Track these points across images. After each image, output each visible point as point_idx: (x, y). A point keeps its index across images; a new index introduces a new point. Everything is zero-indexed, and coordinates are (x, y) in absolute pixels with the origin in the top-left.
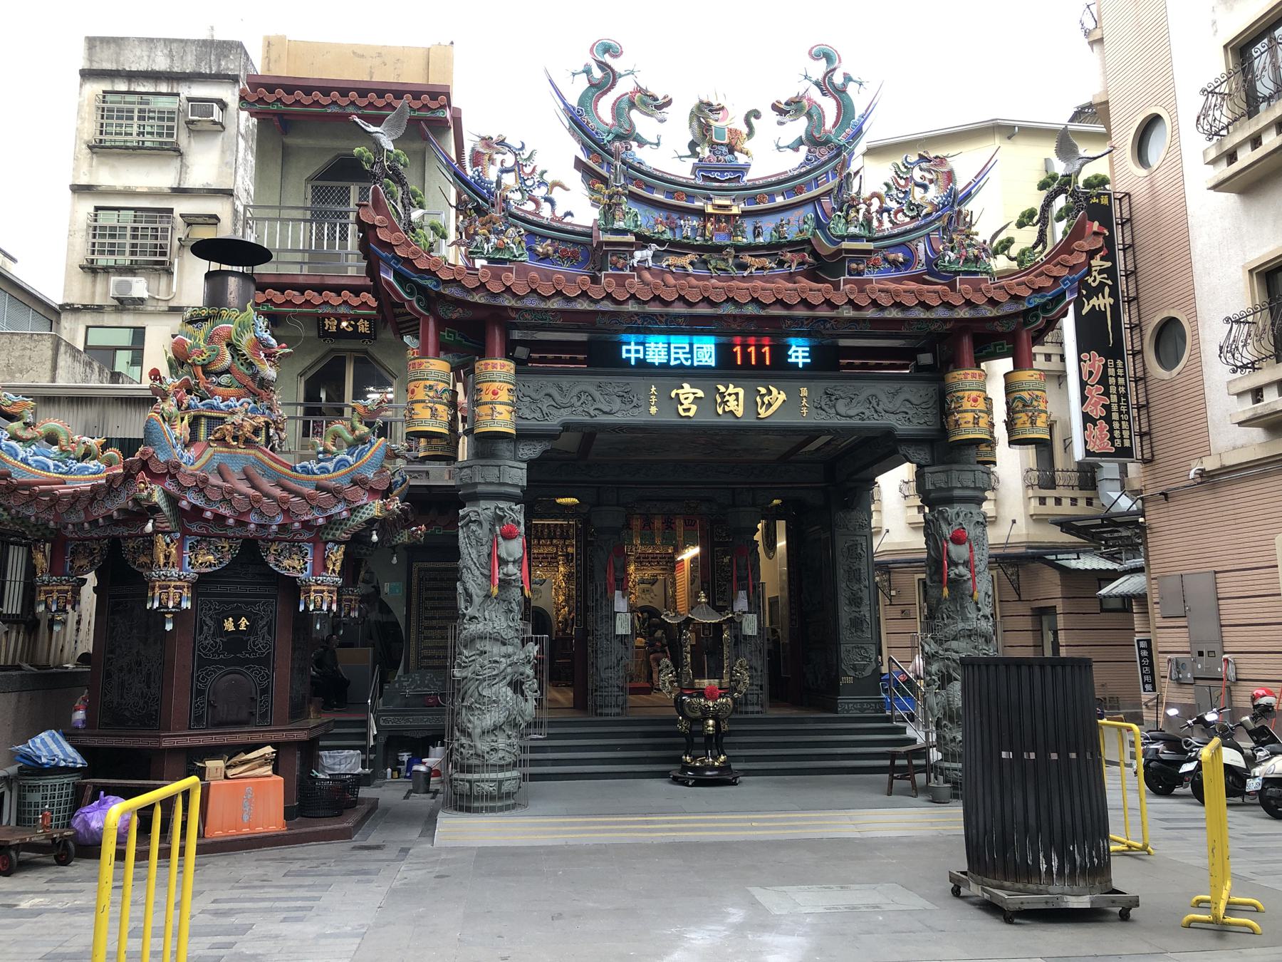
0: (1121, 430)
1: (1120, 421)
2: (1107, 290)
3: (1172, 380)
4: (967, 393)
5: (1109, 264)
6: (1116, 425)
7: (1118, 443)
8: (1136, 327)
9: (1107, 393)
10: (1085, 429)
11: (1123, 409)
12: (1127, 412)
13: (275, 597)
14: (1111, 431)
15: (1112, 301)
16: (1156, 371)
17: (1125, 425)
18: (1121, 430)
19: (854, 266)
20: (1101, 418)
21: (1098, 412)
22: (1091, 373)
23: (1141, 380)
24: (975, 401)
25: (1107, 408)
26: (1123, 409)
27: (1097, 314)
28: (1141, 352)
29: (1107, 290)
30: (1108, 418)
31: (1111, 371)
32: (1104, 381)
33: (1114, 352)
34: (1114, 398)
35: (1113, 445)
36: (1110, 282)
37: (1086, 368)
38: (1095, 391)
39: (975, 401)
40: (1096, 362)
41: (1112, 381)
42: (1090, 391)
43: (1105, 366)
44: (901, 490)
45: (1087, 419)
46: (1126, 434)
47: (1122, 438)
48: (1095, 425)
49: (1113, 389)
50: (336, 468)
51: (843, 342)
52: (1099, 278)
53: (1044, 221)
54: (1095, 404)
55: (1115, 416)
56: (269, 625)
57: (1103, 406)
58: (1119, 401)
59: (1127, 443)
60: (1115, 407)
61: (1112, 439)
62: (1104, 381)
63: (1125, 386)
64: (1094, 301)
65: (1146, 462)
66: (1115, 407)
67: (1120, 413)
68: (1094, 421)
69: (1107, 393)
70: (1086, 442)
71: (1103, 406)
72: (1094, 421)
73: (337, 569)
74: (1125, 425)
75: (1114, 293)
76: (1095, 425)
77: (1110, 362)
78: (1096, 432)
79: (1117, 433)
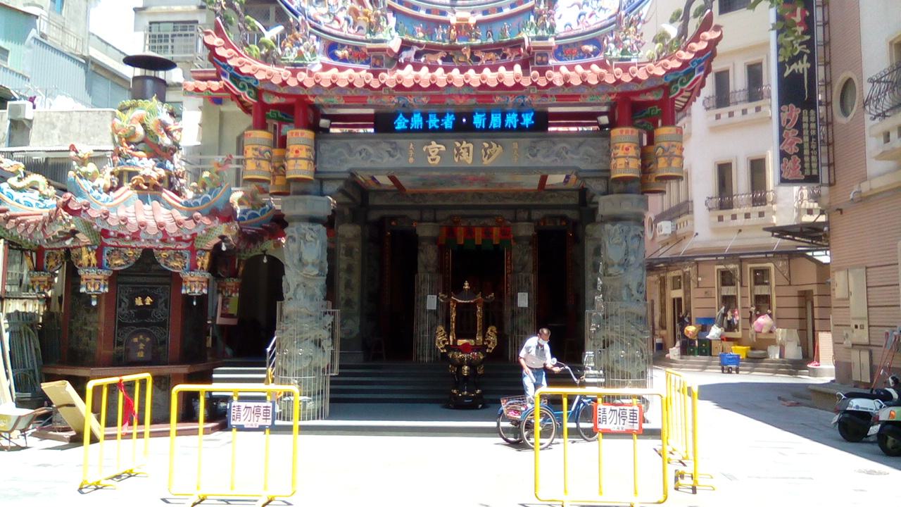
0: (810, 162)
1: (810, 155)
2: (805, 57)
3: (848, 125)
4: (622, 144)
5: (807, 37)
6: (807, 159)
7: (807, 172)
8: (828, 84)
9: (800, 135)
10: (781, 162)
11: (814, 147)
12: (817, 149)
13: (169, 284)
14: (803, 163)
15: (809, 65)
16: (840, 119)
17: (814, 158)
18: (810, 162)
19: (539, 58)
20: (795, 154)
21: (793, 149)
22: (788, 121)
23: (829, 123)
24: (627, 149)
25: (801, 146)
26: (814, 147)
27: (796, 77)
28: (831, 103)
29: (805, 57)
30: (800, 154)
31: (805, 119)
32: (799, 126)
33: (810, 104)
34: (806, 139)
35: (803, 174)
36: (808, 51)
37: (785, 116)
38: (791, 134)
39: (627, 149)
40: (794, 111)
41: (805, 126)
42: (787, 134)
43: (801, 116)
45: (783, 155)
46: (814, 165)
47: (811, 168)
48: (789, 159)
49: (806, 132)
50: (202, 203)
51: (551, 110)
52: (799, 49)
53: (686, 19)
54: (791, 144)
55: (806, 152)
56: (166, 302)
57: (797, 145)
58: (810, 140)
59: (815, 172)
60: (806, 146)
61: (803, 169)
62: (799, 126)
63: (816, 129)
64: (794, 66)
65: (830, 185)
66: (806, 146)
67: (811, 150)
68: (789, 157)
69: (800, 135)
70: (781, 172)
71: (797, 145)
72: (789, 157)
73: (205, 266)
74: (814, 158)
75: (811, 59)
76: (789, 159)
77: (805, 112)
78: (790, 164)
79: (807, 165)
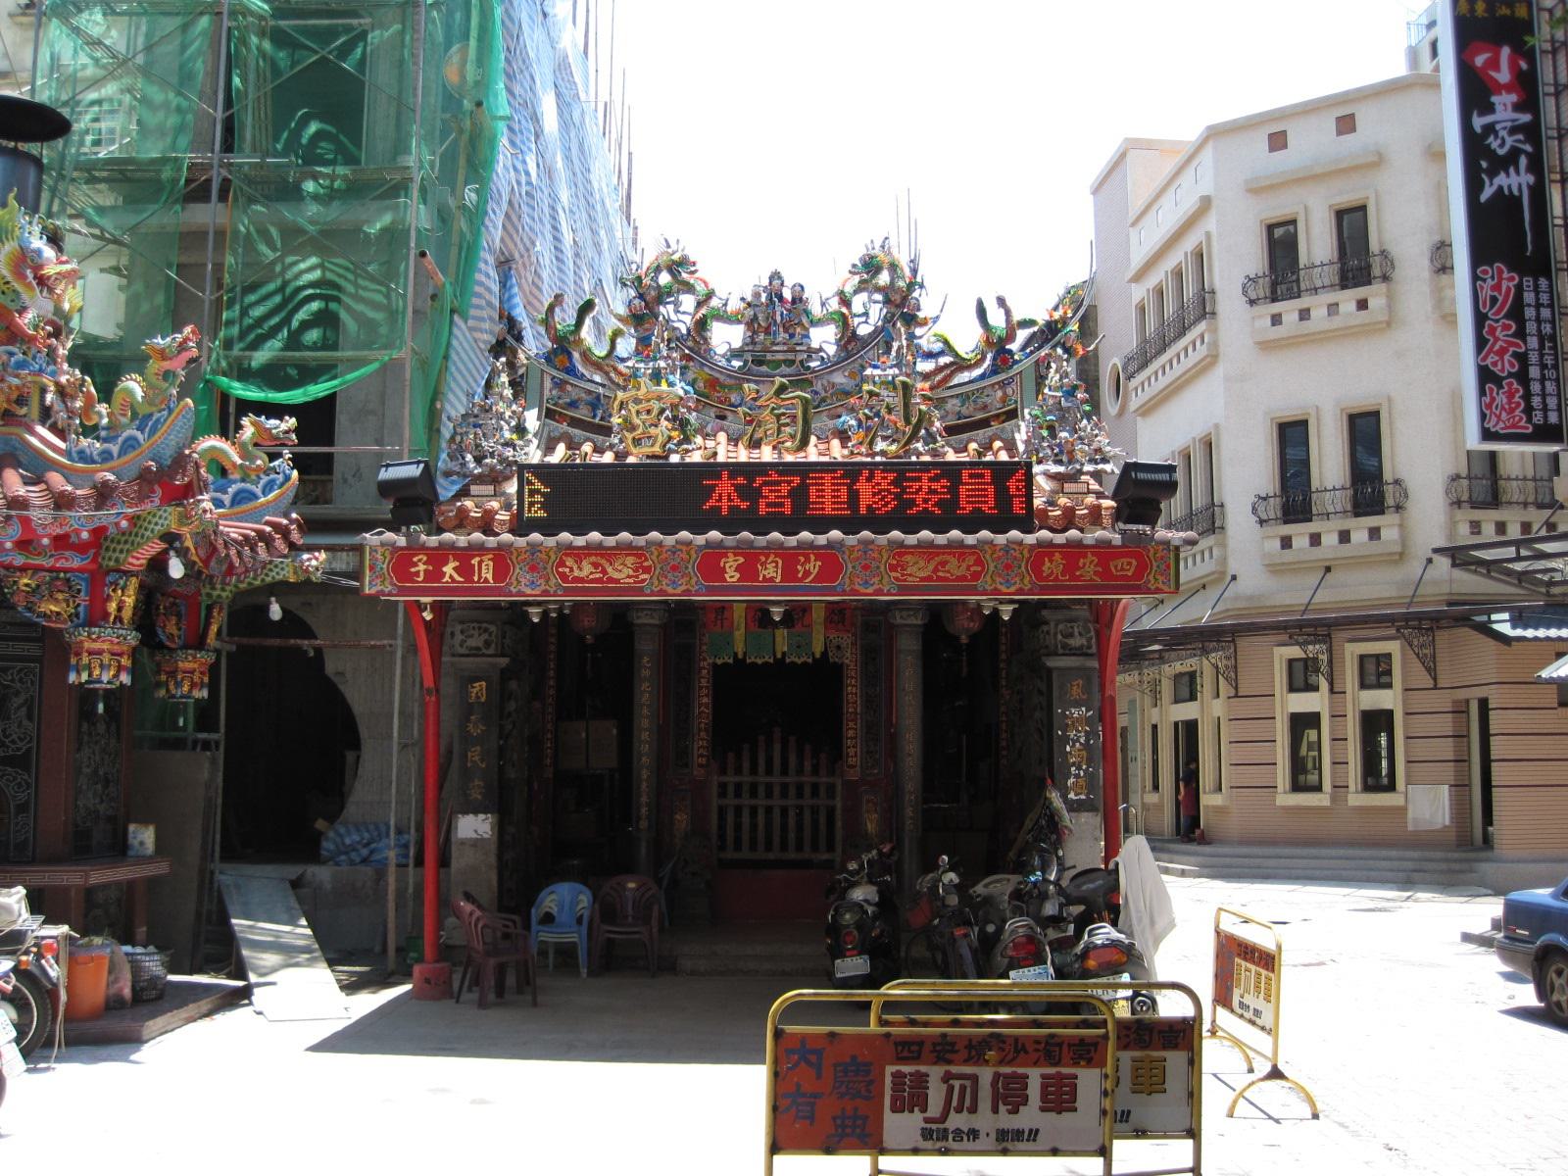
0: (1544, 395)
1: (1543, 380)
2: (1523, 161)
5: (1526, 118)
6: (1535, 387)
7: (1538, 418)
10: (1482, 392)
11: (1549, 360)
12: (1556, 367)
13: (38, 660)
14: (1527, 396)
15: (1531, 179)
17: (1550, 387)
18: (1544, 395)
20: (1510, 375)
21: (1507, 366)
25: (1522, 359)
26: (1549, 360)
27: (1506, 202)
29: (1523, 161)
31: (1529, 297)
32: (1516, 312)
34: (1533, 342)
35: (1529, 420)
36: (1528, 148)
41: (1530, 313)
42: (1492, 330)
43: (1519, 289)
44: (1254, 510)
46: (1552, 402)
47: (1545, 409)
48: (1500, 387)
49: (1531, 327)
50: (123, 452)
52: (1510, 141)
54: (1502, 352)
55: (1534, 372)
56: (29, 704)
57: (1516, 355)
58: (1542, 346)
59: (1553, 418)
60: (1534, 357)
61: (1529, 410)
63: (1553, 322)
64: (1501, 180)
67: (1543, 367)
68: (1498, 381)
69: (1521, 334)
71: (1516, 355)
72: (1498, 381)
73: (127, 614)
74: (1550, 387)
75: (1536, 165)
77: (1528, 282)
79: (1536, 401)
